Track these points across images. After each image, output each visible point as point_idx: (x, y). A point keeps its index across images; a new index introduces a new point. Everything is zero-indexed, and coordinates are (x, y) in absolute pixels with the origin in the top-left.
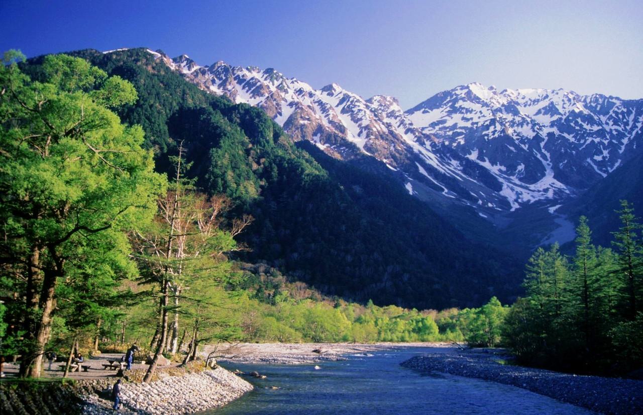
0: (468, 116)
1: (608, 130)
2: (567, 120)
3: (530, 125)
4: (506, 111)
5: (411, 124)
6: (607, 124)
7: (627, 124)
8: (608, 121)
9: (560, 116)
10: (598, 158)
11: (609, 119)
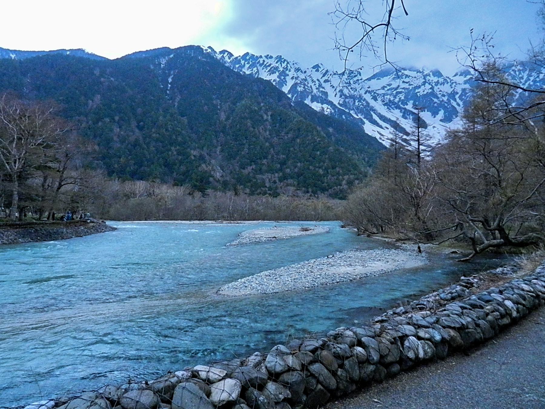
7: (522, 78)
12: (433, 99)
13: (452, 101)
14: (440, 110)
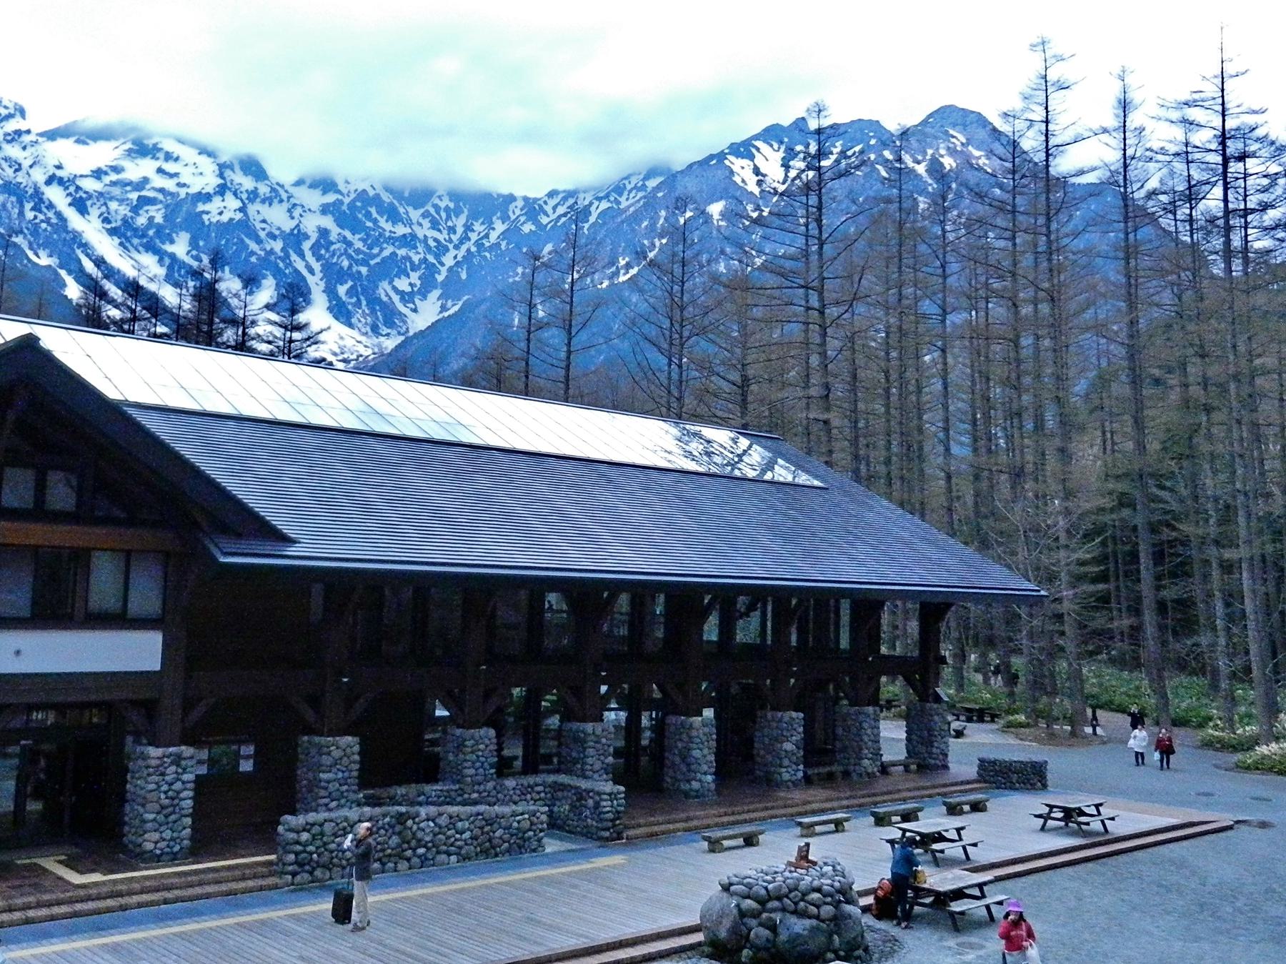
0: (170, 167)
1: (420, 236)
2: (352, 205)
3: (285, 206)
4: (242, 169)
5: (59, 167)
6: (420, 225)
7: (452, 230)
8: (421, 220)
9: (340, 197)
10: (402, 284)
11: (424, 216)
12: (247, 241)
13: (294, 257)
14: (264, 277)
